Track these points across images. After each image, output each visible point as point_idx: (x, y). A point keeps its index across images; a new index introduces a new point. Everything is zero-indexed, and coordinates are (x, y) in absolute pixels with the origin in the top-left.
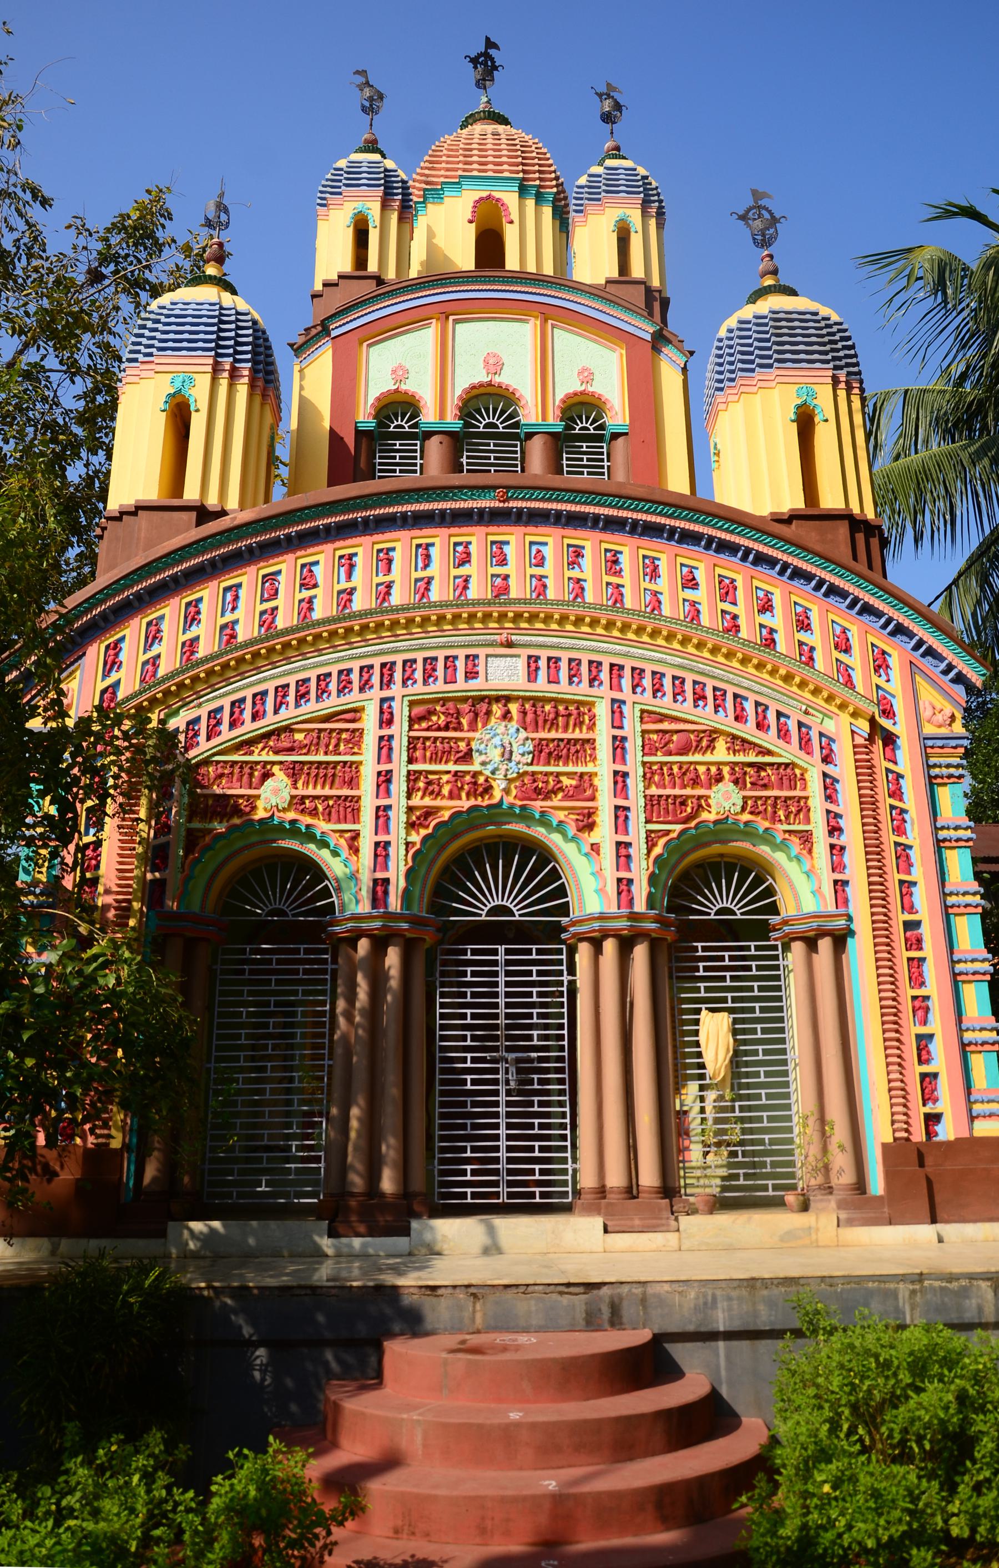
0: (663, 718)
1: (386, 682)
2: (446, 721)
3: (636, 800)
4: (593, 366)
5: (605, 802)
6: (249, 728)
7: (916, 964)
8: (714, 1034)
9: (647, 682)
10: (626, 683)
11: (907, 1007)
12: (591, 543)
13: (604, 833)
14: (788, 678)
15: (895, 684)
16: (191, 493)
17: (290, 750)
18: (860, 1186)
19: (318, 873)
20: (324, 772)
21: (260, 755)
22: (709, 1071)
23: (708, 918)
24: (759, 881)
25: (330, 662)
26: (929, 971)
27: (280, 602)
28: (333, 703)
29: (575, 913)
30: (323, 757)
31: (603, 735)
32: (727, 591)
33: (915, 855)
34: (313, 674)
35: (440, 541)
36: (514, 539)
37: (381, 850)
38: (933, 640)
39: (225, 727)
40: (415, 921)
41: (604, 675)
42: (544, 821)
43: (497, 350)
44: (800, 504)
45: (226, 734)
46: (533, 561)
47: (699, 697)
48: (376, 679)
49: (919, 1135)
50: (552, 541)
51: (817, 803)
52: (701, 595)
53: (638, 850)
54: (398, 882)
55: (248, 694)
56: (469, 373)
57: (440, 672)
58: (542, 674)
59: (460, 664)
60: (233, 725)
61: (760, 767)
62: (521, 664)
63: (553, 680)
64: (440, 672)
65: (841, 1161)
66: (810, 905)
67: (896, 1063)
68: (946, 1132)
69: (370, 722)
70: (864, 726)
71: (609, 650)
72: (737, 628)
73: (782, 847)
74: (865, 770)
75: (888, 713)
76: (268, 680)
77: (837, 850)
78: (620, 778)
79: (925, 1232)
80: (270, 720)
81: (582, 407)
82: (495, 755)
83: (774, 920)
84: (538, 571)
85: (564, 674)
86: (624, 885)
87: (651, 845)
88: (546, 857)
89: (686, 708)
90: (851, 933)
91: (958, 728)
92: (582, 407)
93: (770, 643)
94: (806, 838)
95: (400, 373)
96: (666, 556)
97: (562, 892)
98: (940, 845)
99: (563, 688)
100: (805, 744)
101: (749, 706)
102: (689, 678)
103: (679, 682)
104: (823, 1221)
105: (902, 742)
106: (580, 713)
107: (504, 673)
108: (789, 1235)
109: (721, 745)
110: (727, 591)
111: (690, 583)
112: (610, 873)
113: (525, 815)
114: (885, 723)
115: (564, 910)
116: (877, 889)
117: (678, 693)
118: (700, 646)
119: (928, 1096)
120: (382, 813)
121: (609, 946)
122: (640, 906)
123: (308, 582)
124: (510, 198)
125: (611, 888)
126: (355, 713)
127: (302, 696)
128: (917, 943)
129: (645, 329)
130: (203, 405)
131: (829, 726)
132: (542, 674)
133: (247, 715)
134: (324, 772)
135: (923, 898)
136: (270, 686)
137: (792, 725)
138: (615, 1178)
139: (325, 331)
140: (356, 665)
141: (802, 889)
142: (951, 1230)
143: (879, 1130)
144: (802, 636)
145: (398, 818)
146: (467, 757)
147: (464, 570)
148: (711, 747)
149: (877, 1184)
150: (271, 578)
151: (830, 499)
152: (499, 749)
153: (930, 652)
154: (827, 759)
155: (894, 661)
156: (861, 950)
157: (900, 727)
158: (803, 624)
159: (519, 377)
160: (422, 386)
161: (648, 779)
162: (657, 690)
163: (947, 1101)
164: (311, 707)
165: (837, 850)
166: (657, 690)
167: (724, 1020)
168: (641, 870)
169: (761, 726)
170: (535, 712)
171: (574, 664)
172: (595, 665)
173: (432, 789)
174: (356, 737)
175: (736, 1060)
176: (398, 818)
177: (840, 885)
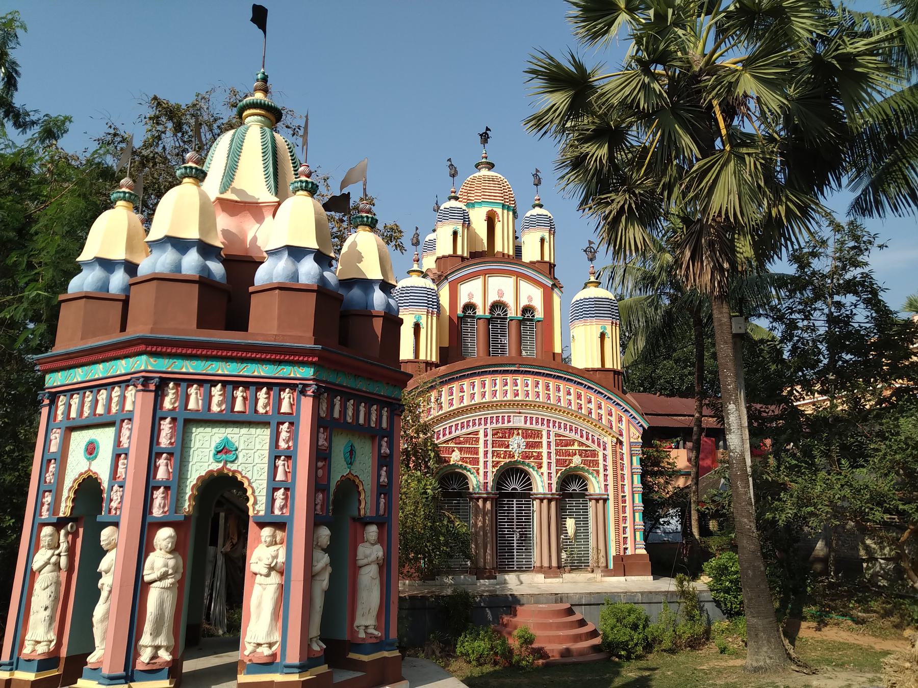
0: (561, 436)
1: (486, 424)
2: (503, 435)
3: (553, 460)
4: (532, 295)
5: (545, 461)
6: (448, 437)
8: (570, 524)
10: (551, 425)
12: (541, 380)
13: (544, 469)
14: (595, 426)
15: (624, 426)
17: (459, 443)
18: (607, 566)
19: (466, 478)
20: (469, 451)
21: (451, 445)
23: (571, 490)
24: (583, 481)
25: (470, 416)
28: (471, 429)
29: (534, 491)
30: (468, 443)
32: (579, 397)
33: (626, 477)
34: (465, 421)
35: (499, 379)
36: (520, 379)
37: (486, 473)
38: (635, 415)
39: (441, 436)
40: (495, 494)
41: (545, 422)
42: (528, 465)
43: (500, 287)
44: (599, 366)
45: (442, 439)
46: (525, 387)
47: (571, 430)
48: (483, 422)
49: (622, 553)
50: (530, 380)
52: (572, 398)
53: (553, 475)
54: (490, 484)
55: (447, 426)
56: (492, 298)
58: (528, 422)
59: (506, 418)
60: (444, 435)
61: (586, 451)
62: (523, 419)
63: (531, 424)
65: (602, 560)
66: (597, 491)
67: (617, 534)
68: (629, 552)
70: (615, 440)
71: (547, 415)
72: (581, 408)
73: (592, 474)
74: (614, 452)
75: (621, 435)
76: (453, 422)
77: (606, 476)
78: (549, 453)
79: (622, 579)
80: (454, 435)
82: (516, 446)
83: (587, 493)
84: (526, 389)
86: (550, 485)
88: (527, 474)
89: (567, 433)
90: (608, 499)
91: (640, 440)
92: (528, 309)
93: (590, 413)
94: (598, 472)
95: (471, 295)
96: (562, 385)
97: (530, 484)
98: (632, 474)
99: (534, 426)
100: (599, 445)
101: (584, 433)
102: (569, 424)
103: (565, 425)
104: (598, 575)
105: (625, 444)
106: (538, 434)
107: (518, 422)
109: (576, 444)
110: (579, 397)
111: (569, 393)
113: (523, 463)
114: (620, 438)
115: (531, 489)
117: (565, 428)
119: (625, 543)
120: (485, 463)
121: (545, 501)
122: (554, 491)
123: (462, 391)
124: (499, 210)
125: (547, 486)
126: (477, 433)
127: (462, 427)
128: (624, 502)
129: (549, 283)
130: (425, 326)
131: (605, 439)
132: (528, 422)
133: (447, 432)
134: (469, 451)
135: (626, 488)
136: (454, 424)
137: (596, 439)
138: (546, 564)
139: (446, 278)
140: (477, 418)
141: (595, 486)
142: (628, 578)
143: (613, 552)
144: (599, 411)
145: (490, 464)
146: (508, 447)
147: (506, 388)
149: (611, 566)
150: (451, 388)
151: (608, 365)
152: (517, 444)
153: (634, 417)
154: (604, 449)
155: (624, 419)
156: (611, 503)
157: (624, 439)
158: (600, 408)
159: (509, 299)
160: (478, 301)
161: (556, 454)
162: (560, 427)
163: (629, 545)
164: (465, 431)
165: (606, 476)
166: (560, 427)
167: (573, 521)
168: (554, 480)
169: (587, 439)
171: (537, 419)
172: (543, 420)
173: (498, 456)
174: (477, 440)
175: (576, 532)
176: (490, 464)
177: (606, 486)
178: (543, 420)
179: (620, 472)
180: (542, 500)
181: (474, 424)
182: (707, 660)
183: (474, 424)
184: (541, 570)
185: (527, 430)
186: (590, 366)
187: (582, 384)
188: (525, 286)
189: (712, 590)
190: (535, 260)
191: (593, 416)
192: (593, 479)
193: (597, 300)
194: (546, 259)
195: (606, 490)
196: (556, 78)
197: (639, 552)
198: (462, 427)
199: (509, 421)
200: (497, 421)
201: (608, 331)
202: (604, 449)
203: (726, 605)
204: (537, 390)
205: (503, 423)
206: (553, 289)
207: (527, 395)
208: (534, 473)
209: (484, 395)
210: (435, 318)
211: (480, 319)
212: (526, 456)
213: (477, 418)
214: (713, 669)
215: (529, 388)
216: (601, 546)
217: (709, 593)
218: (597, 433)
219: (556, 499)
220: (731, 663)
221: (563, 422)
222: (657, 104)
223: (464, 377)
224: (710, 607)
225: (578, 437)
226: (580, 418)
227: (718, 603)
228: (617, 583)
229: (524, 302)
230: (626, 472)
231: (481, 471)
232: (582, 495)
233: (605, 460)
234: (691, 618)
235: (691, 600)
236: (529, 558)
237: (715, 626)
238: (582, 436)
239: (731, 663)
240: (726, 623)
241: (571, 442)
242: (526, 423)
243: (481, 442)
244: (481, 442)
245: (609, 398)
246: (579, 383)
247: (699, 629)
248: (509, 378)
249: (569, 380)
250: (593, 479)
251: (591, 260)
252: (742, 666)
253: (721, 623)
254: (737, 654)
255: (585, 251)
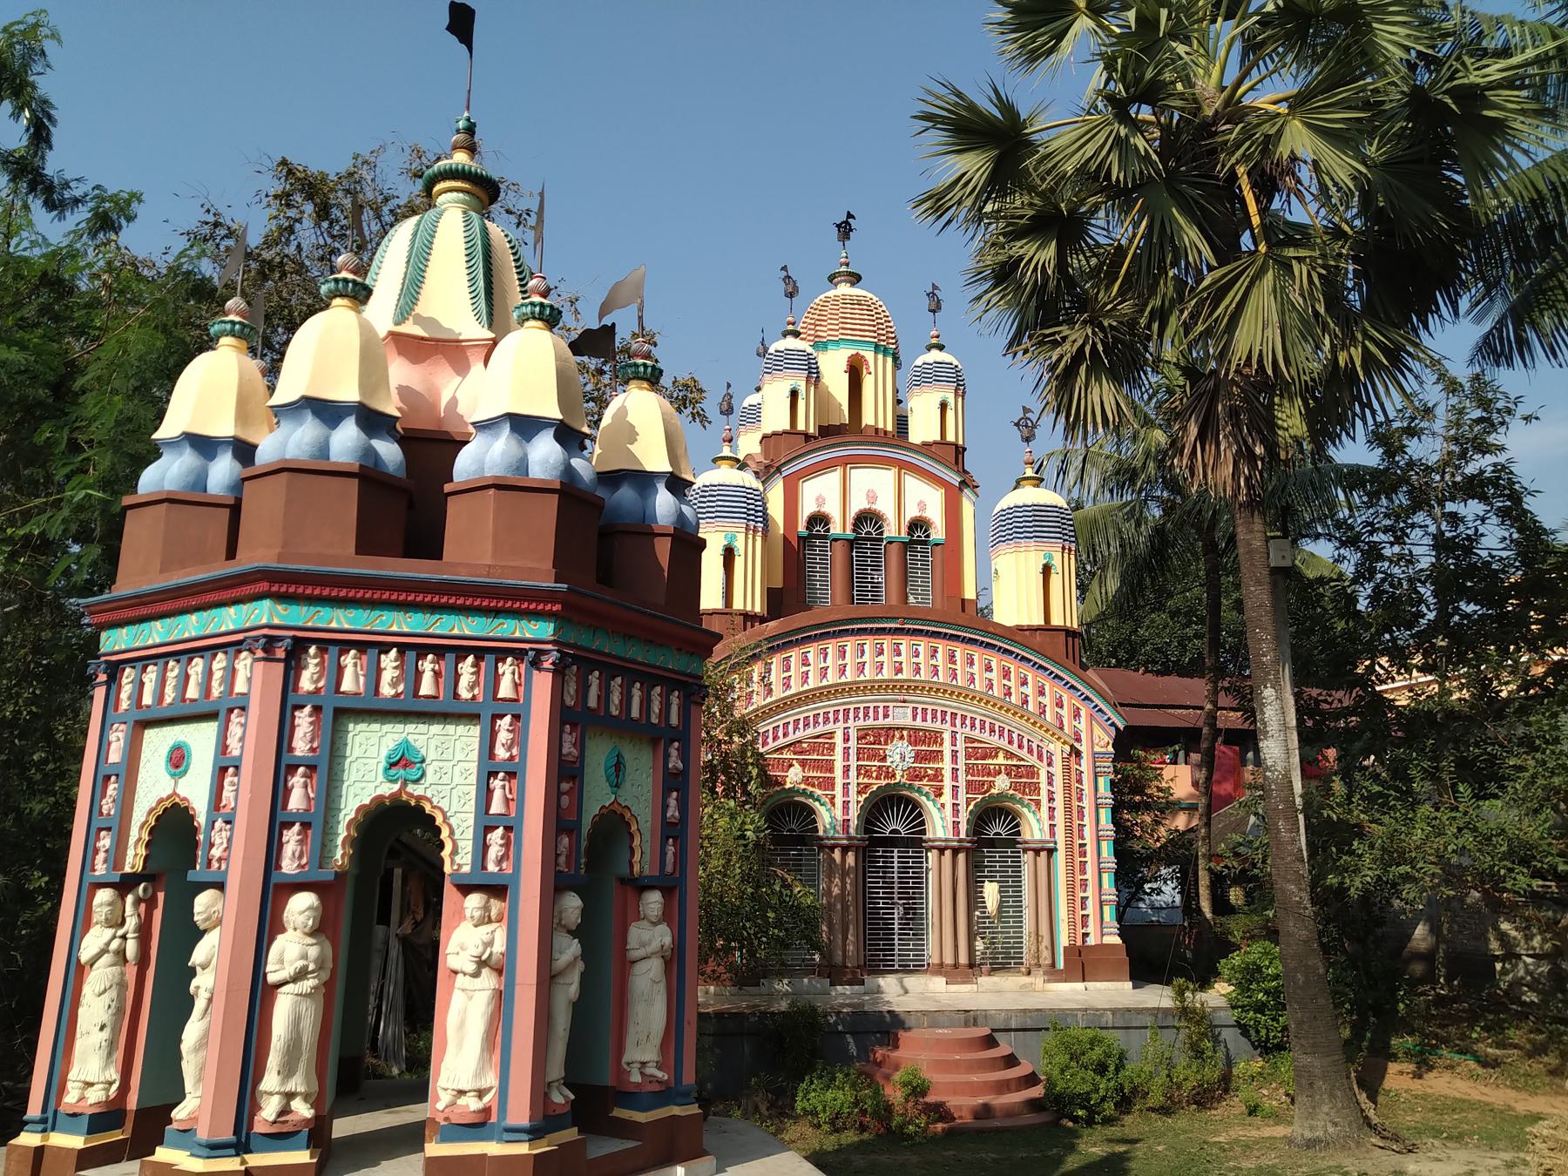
0: (975, 741)
1: (846, 721)
3: (962, 783)
4: (925, 500)
5: (947, 783)
6: (781, 741)
7: (1083, 864)
8: (991, 891)
9: (968, 722)
10: (958, 722)
11: (1078, 884)
12: (941, 646)
13: (947, 798)
14: (1034, 724)
15: (1082, 725)
16: (738, 604)
17: (801, 753)
18: (1053, 965)
19: (812, 811)
20: (817, 765)
21: (787, 755)
22: (989, 909)
23: (991, 834)
24: (1013, 819)
25: (821, 707)
26: (1089, 867)
27: (792, 673)
28: (820, 729)
29: (929, 835)
30: (816, 752)
31: (947, 748)
32: (1006, 674)
33: (1086, 812)
34: (811, 714)
35: (869, 643)
36: (905, 643)
37: (846, 804)
39: (770, 740)
41: (948, 718)
42: (919, 791)
45: (772, 745)
46: (914, 657)
47: (992, 731)
48: (841, 716)
49: (1079, 943)
50: (923, 645)
51: (1044, 787)
52: (993, 675)
54: (854, 823)
55: (781, 723)
56: (858, 504)
57: (871, 714)
58: (919, 717)
59: (881, 710)
62: (909, 711)
63: (924, 720)
64: (871, 714)
65: (1046, 954)
66: (1038, 836)
68: (1091, 941)
69: (838, 739)
70: (1067, 748)
71: (951, 705)
73: (1028, 806)
74: (1067, 769)
75: (1079, 740)
76: (790, 716)
78: (954, 771)
79: (1080, 986)
80: (791, 738)
81: (919, 525)
83: (1019, 839)
85: (929, 717)
86: (956, 824)
87: (968, 805)
88: (916, 805)
89: (985, 736)
92: (919, 525)
93: (1026, 702)
94: (1038, 803)
95: (820, 500)
96: (978, 654)
97: (923, 823)
98: (1097, 807)
99: (929, 724)
100: (1040, 757)
102: (988, 721)
103: (983, 723)
104: (1038, 980)
106: (936, 737)
108: (1024, 986)
109: (1001, 754)
110: (1006, 674)
111: (989, 669)
112: (950, 819)
114: (1077, 745)
115: (924, 832)
116: (1069, 829)
117: (983, 727)
118: (994, 705)
119: (1084, 925)
120: (846, 786)
121: (948, 853)
122: (963, 835)
123: (806, 663)
124: (869, 355)
125: (950, 826)
126: (831, 735)
127: (806, 725)
128: (1084, 854)
129: (955, 479)
130: (742, 552)
131: (1051, 747)
132: (919, 717)
133: (780, 734)
134: (817, 765)
136: (791, 720)
138: (949, 960)
139: (779, 470)
141: (1034, 827)
142: (1090, 985)
143: (1063, 940)
144: (1040, 699)
145: (853, 789)
146: (884, 759)
147: (880, 659)
148: (996, 756)
149: (1061, 965)
150: (787, 659)
151: (1057, 620)
152: (899, 754)
154: (1050, 764)
155: (1083, 713)
156: (1060, 857)
157: (1083, 747)
158: (1042, 693)
159: (886, 507)
160: (833, 509)
161: (967, 773)
162: (973, 726)
163: (1091, 929)
164: (811, 731)
166: (973, 726)
167: (995, 886)
168: (963, 817)
169: (1020, 746)
170: (917, 736)
171: (934, 712)
172: (944, 713)
173: (868, 774)
174: (832, 747)
176: (853, 789)
177: (1052, 826)
178: (944, 713)
179: (1075, 803)
180: (942, 851)
181: (826, 720)
182: (1226, 1126)
183: (826, 720)
184: (940, 969)
185: (917, 730)
186: (1025, 622)
187: (1011, 653)
188: (912, 484)
189: (1233, 1008)
190: (930, 439)
191: (1031, 708)
192: (1030, 816)
193: (1038, 510)
194: (950, 437)
195: (1052, 834)
196: (966, 127)
197: (1108, 940)
198: (806, 725)
199: (886, 716)
200: (866, 715)
201: (1056, 562)
202: (1050, 764)
203: (1258, 1032)
204: (933, 662)
205: (876, 718)
206: (961, 490)
207: (918, 671)
208: (929, 805)
209: (843, 671)
210: (759, 540)
211: (836, 540)
212: (916, 775)
213: (831, 710)
214: (1236, 1141)
215: (921, 659)
216: (1044, 930)
217: (1230, 1012)
218: (1036, 737)
219: (967, 849)
220: (1267, 1132)
221: (979, 718)
222: (1141, 172)
223: (809, 640)
224: (1230, 1036)
225: (1003, 743)
226: (1008, 711)
227: (1244, 1030)
228: (1070, 994)
229: (911, 512)
230: (1087, 803)
231: (839, 801)
232: (1012, 843)
233: (1050, 784)
234: (1198, 1053)
235: (1198, 1023)
236: (920, 949)
237: (1240, 1068)
238: (1010, 742)
239: (1267, 1132)
240: (1258, 1064)
241: (992, 752)
242: (914, 718)
243: (839, 750)
244: (839, 750)
245: (1057, 676)
246: (1006, 651)
247: (1212, 1073)
248: (887, 642)
249: (989, 645)
250: (1030, 816)
251: (1027, 440)
252: (1285, 1137)
253: (1249, 1064)
254: (1276, 1117)
255: (1017, 424)
